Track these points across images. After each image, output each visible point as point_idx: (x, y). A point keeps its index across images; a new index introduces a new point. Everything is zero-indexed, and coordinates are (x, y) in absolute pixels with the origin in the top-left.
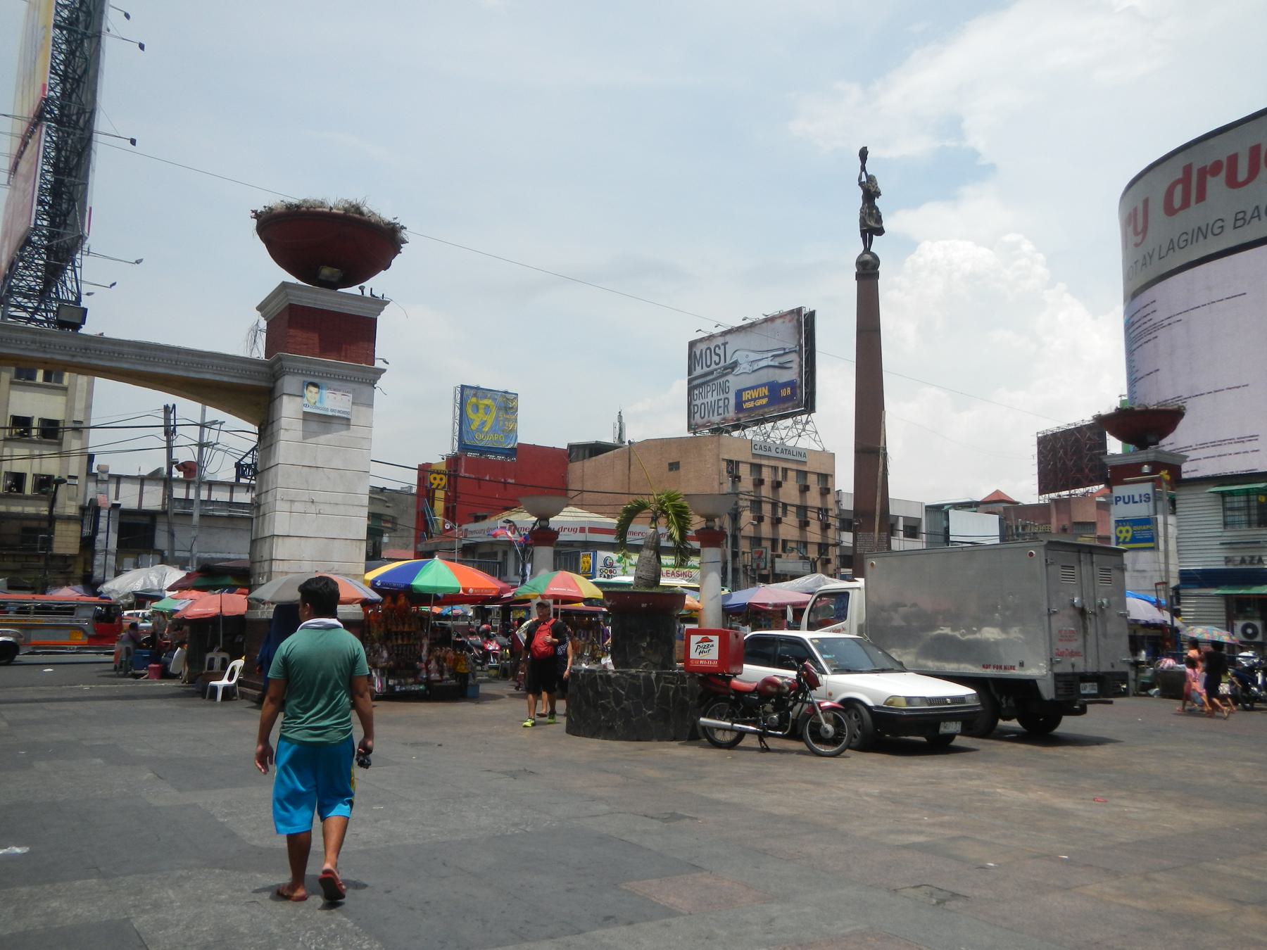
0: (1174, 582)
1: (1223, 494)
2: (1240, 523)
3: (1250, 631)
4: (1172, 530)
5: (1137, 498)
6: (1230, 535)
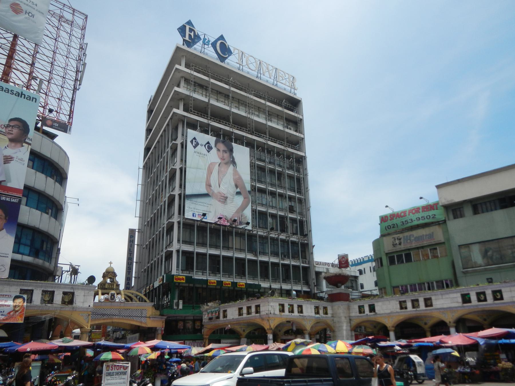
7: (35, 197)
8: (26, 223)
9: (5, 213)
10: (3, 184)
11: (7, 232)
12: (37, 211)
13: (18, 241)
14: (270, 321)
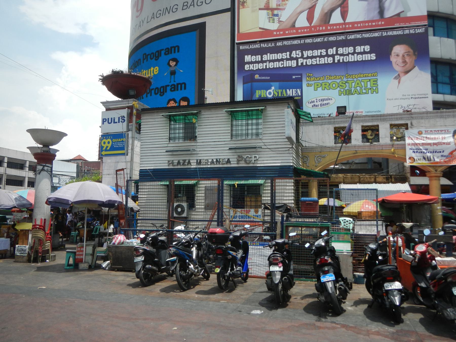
0: (136, 176)
1: (170, 116)
2: (179, 138)
3: (179, 210)
4: (137, 149)
5: (117, 120)
6: (172, 145)
7: (441, 25)
8: (440, 57)
9: (412, 48)
10: (402, 15)
11: (420, 69)
12: (450, 40)
13: (435, 81)
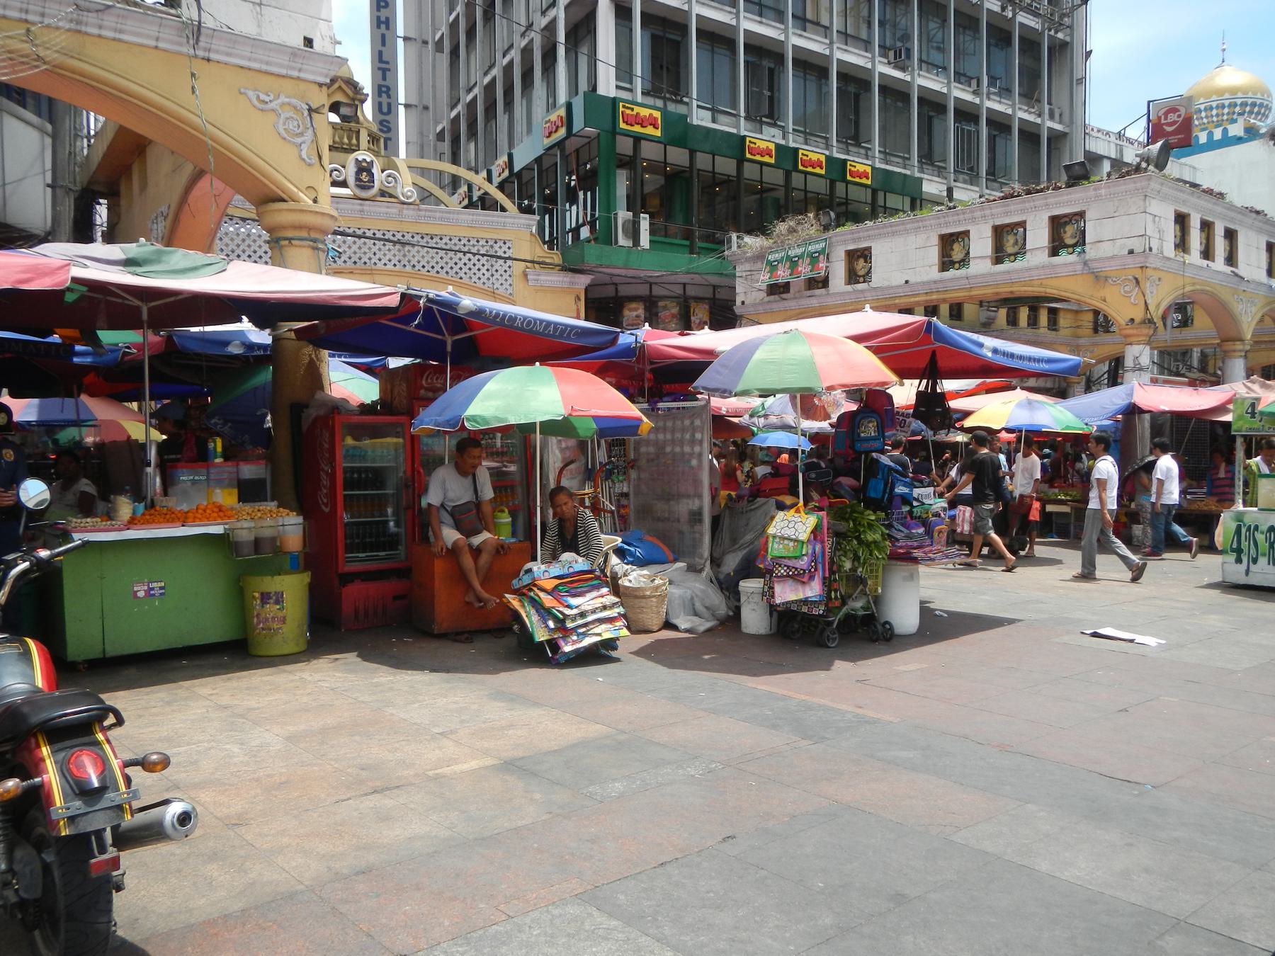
14: (1147, 286)
